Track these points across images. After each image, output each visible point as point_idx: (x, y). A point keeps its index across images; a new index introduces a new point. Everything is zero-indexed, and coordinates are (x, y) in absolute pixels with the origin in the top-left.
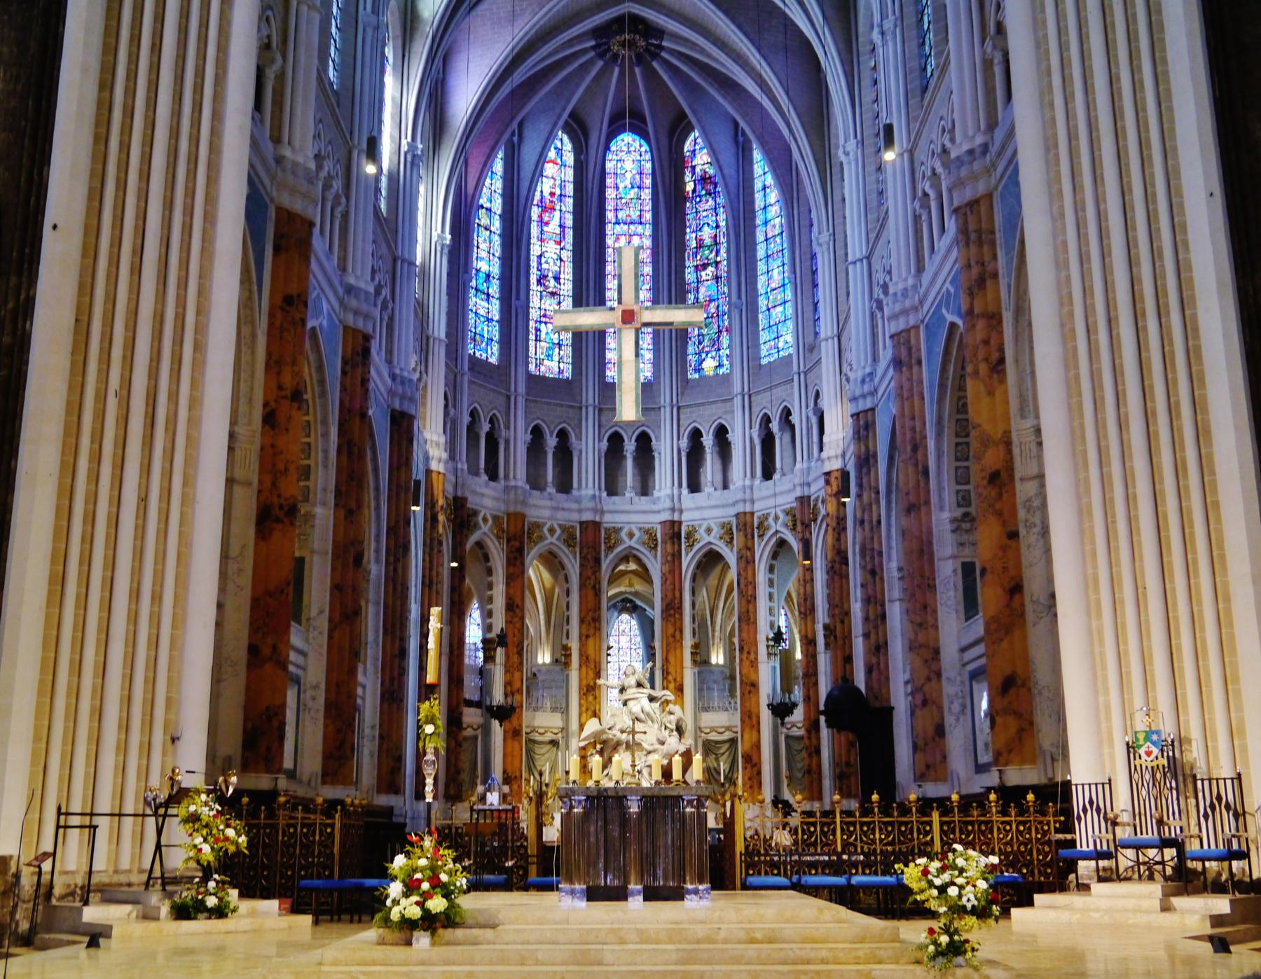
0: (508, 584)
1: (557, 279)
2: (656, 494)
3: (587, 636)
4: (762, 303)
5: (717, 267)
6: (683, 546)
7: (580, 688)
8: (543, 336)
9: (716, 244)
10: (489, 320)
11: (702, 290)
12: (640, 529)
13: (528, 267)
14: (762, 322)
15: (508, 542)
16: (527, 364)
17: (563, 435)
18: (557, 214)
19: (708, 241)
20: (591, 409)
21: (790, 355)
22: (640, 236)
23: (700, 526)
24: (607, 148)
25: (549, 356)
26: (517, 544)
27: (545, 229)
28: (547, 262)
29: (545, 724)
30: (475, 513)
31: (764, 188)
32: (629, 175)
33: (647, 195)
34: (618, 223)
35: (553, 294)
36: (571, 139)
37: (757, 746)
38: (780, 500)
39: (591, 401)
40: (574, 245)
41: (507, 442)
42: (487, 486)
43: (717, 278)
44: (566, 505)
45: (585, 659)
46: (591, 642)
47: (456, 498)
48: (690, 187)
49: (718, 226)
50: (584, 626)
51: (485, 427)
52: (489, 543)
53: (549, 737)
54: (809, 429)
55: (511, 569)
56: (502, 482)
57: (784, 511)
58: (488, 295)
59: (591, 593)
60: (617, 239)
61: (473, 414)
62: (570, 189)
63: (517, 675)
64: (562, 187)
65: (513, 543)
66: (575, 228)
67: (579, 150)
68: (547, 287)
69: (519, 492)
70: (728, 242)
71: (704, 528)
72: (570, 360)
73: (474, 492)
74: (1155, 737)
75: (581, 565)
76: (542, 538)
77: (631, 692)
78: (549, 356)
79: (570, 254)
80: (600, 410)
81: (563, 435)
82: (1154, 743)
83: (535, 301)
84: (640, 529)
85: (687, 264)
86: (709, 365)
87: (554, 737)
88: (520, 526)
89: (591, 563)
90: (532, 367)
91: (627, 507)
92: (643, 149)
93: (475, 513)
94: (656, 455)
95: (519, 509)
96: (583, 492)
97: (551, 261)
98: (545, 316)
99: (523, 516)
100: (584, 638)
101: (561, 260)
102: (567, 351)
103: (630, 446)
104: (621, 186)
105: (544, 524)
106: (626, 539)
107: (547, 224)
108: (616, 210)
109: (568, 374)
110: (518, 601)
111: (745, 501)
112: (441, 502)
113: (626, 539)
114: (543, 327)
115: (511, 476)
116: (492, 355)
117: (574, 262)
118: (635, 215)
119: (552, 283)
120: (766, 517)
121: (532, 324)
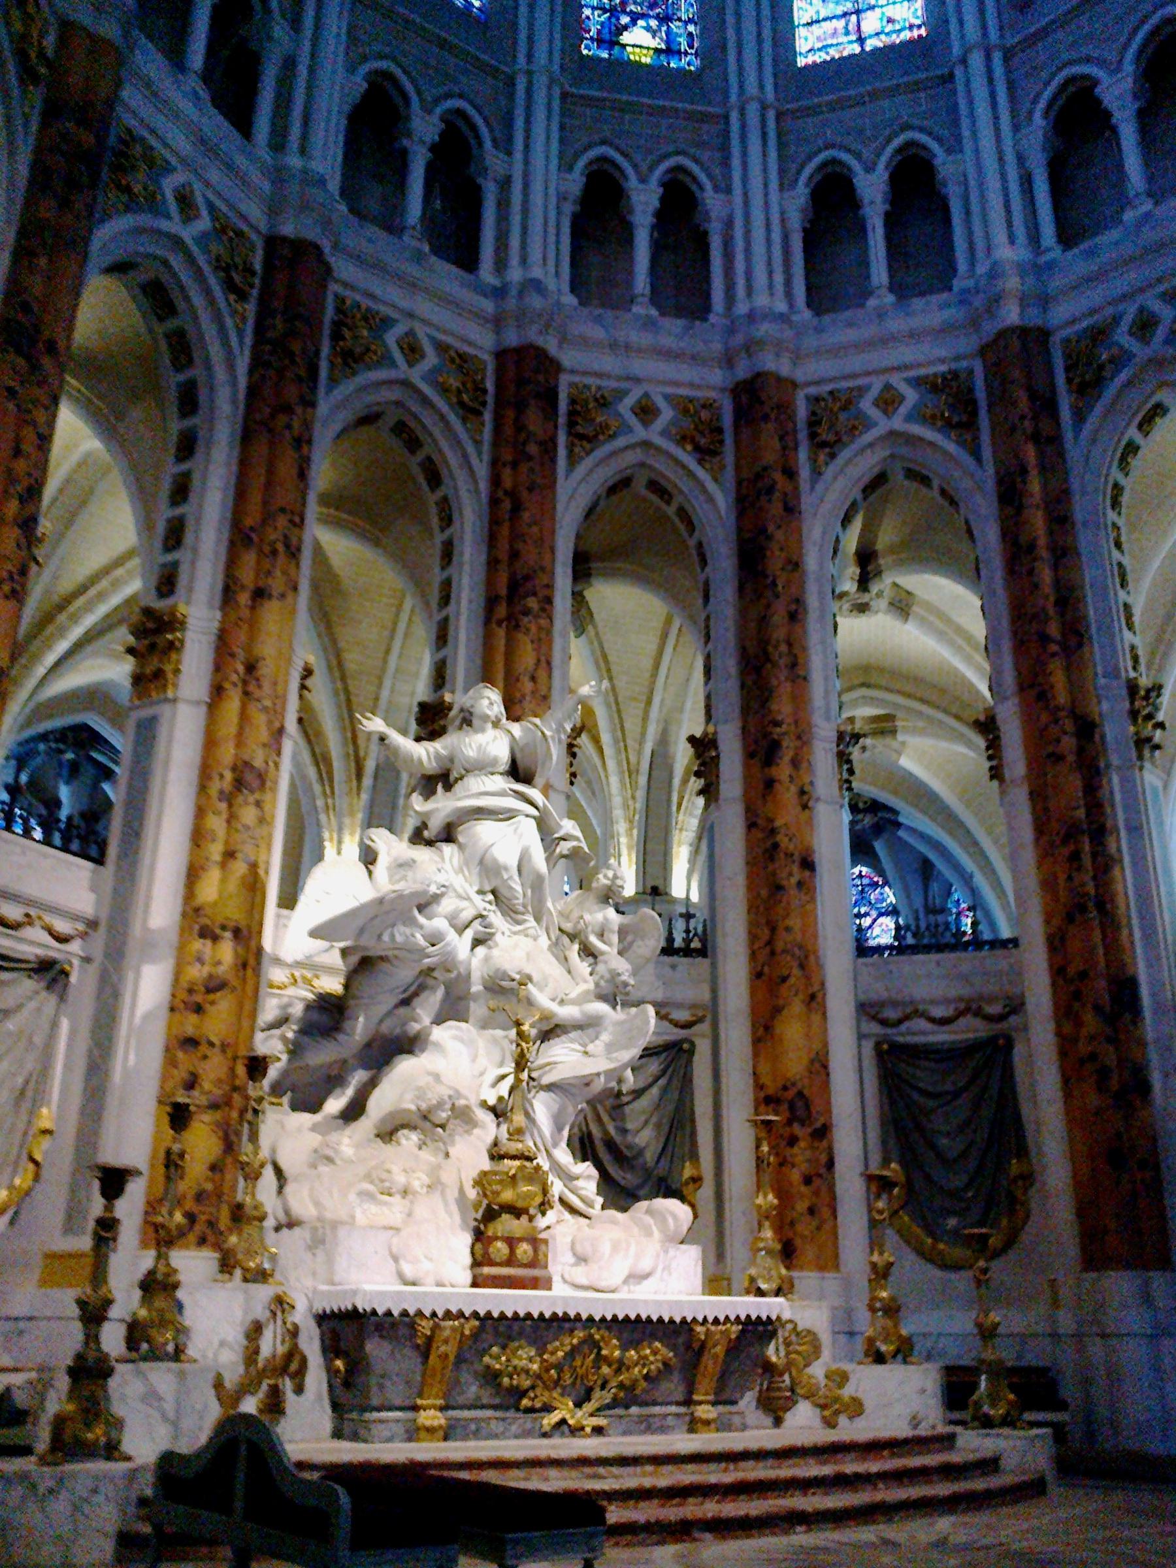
3: (260, 594)
6: (562, 438)
12: (442, 348)
23: (621, 394)
29: (31, 888)
37: (820, 1065)
38: (905, 353)
50: (249, 559)
53: (32, 944)
54: (1027, 181)
57: (917, 382)
71: (630, 401)
77: (488, 788)
87: (54, 950)
111: (779, 347)
120: (847, 401)
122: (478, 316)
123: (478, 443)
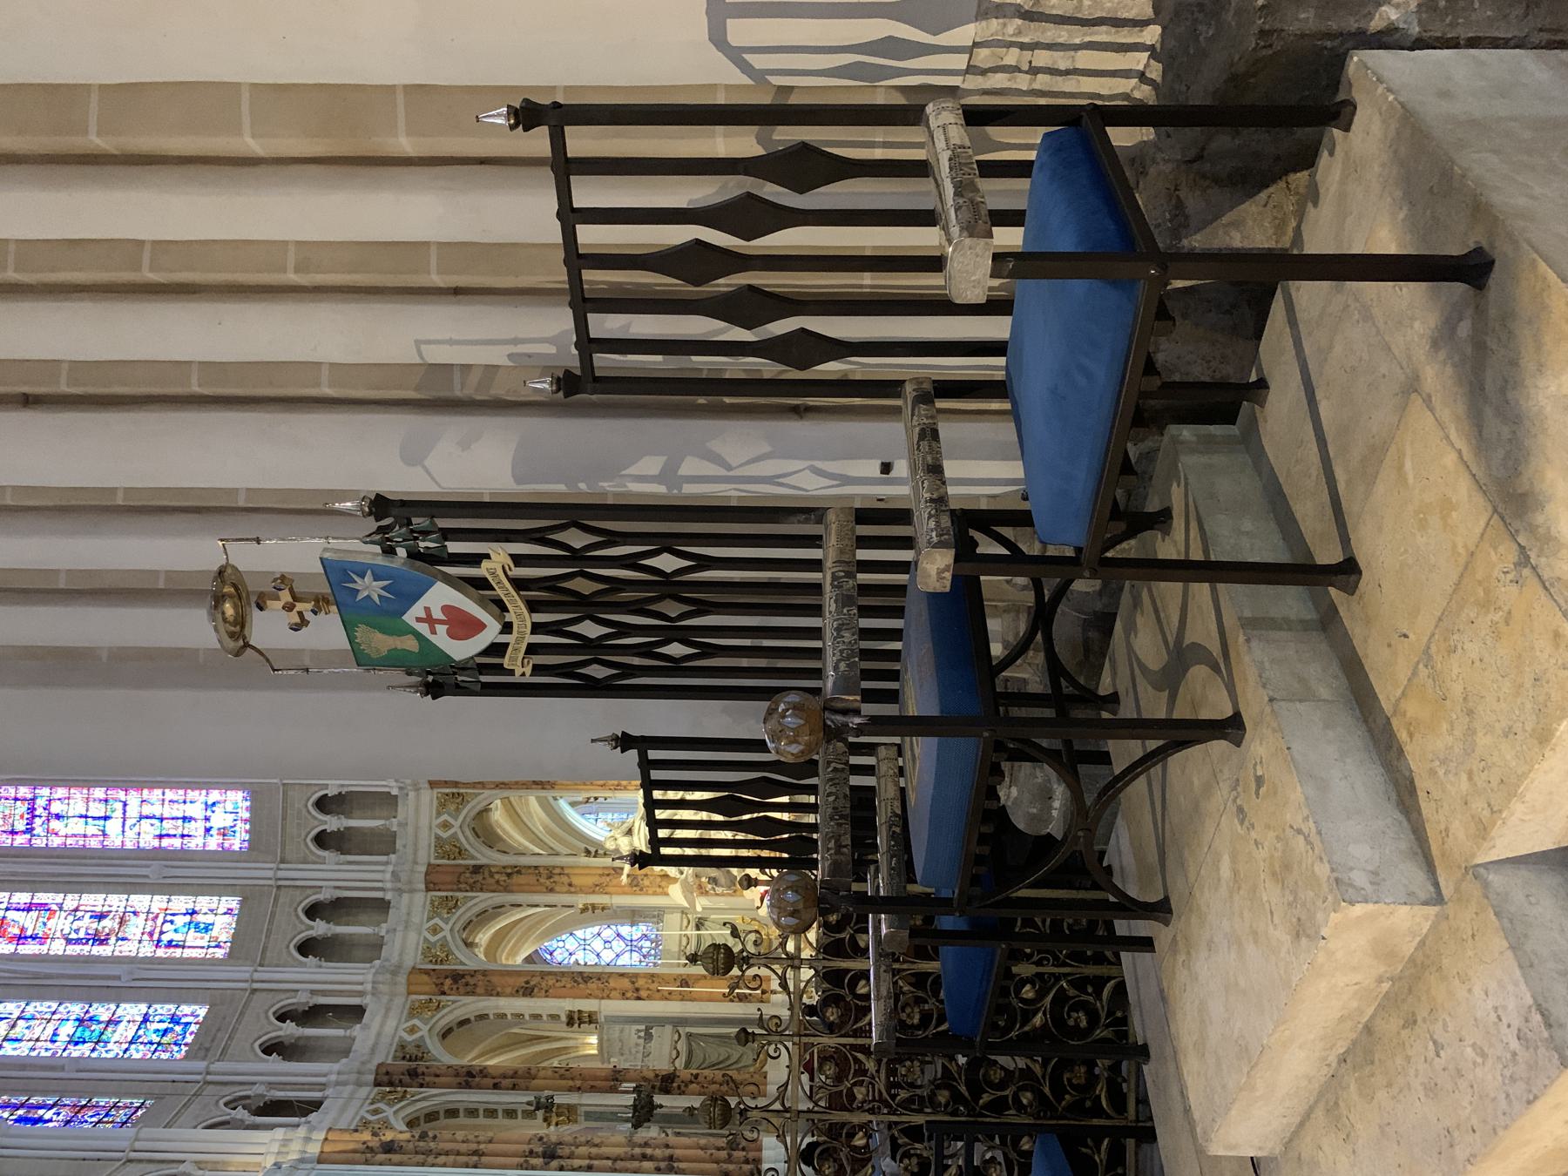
0: (498, 995)
1: (101, 917)
2: (394, 792)
7: (634, 893)
8: (178, 937)
10: (146, 1019)
12: (439, 814)
15: (444, 993)
17: (313, 911)
20: (281, 874)
25: (207, 928)
26: (448, 982)
28: (77, 931)
30: (402, 1046)
34: (30, 830)
35: (122, 922)
39: (270, 874)
41: (313, 992)
42: (367, 1027)
44: (404, 910)
45: (597, 888)
46: (576, 881)
47: (377, 1084)
51: (290, 1029)
52: (443, 1022)
55: (478, 990)
56: (366, 1001)
58: (109, 1022)
59: (516, 879)
61: (268, 1050)
63: (612, 984)
65: (446, 988)
68: (112, 930)
69: (380, 978)
72: (215, 899)
73: (373, 1050)
74: (370, 588)
75: (481, 890)
76: (444, 944)
78: (207, 928)
79: (70, 896)
80: (283, 861)
81: (313, 911)
82: (406, 595)
84: (439, 814)
87: (693, 924)
88: (425, 978)
89: (478, 878)
90: (219, 953)
91: (410, 829)
93: (402, 1046)
94: (344, 790)
95: (402, 979)
96: (389, 885)
97: (76, 925)
98: (151, 934)
99: (414, 971)
100: (571, 888)
101: (76, 910)
102: (203, 902)
103: (332, 823)
105: (426, 940)
106: (450, 832)
109: (233, 902)
110: (521, 981)
112: (366, 1136)
113: (450, 832)
114: (165, 938)
115: (359, 988)
118: (22, 808)
119: (107, 923)
121: (161, 953)
122: (418, 797)
123: (477, 795)
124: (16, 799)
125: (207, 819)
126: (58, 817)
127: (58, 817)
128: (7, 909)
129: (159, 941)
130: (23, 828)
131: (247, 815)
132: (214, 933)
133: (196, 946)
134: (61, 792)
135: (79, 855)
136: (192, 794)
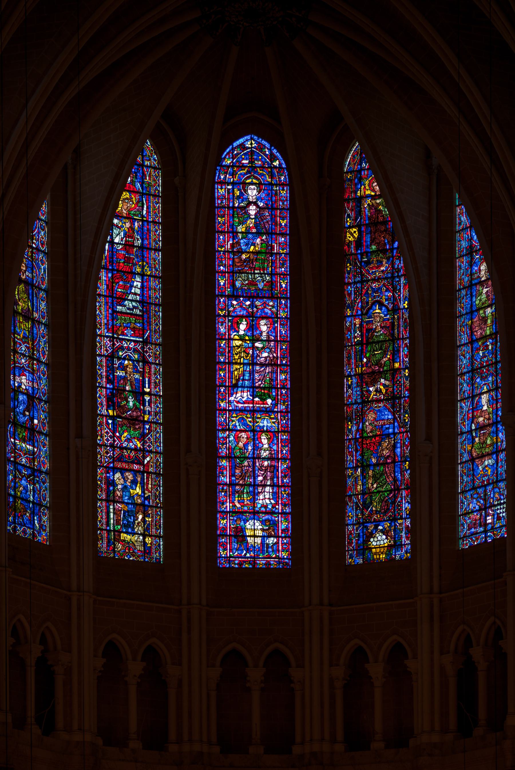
1: (139, 395)
4: (464, 448)
5: (393, 380)
9: (394, 339)
11: (371, 416)
13: (94, 375)
14: (463, 480)
16: (96, 540)
18: (137, 283)
19: (380, 334)
21: (502, 538)
22: (272, 319)
24: (219, 161)
27: (119, 308)
28: (123, 368)
31: (471, 251)
32: (252, 210)
33: (281, 245)
36: (158, 148)
40: (165, 334)
43: (392, 398)
48: (352, 235)
49: (396, 309)
60: (234, 327)
62: (156, 234)
64: (144, 234)
66: (165, 305)
67: (169, 168)
68: (124, 409)
70: (411, 338)
79: (159, 350)
83: (104, 436)
85: (347, 371)
86: (380, 540)
90: (102, 545)
92: (276, 164)
98: (120, 459)
101: (145, 362)
104: (241, 229)
107: (121, 299)
108: (232, 273)
116: (41, 528)
117: (164, 364)
124: (271, 275)
125: (255, 514)
126: (252, 327)
127: (252, 327)
128: (142, 275)
129: (115, 470)
130: (238, 284)
131: (261, 563)
132: (123, 536)
133: (109, 516)
134: (283, 331)
135: (210, 364)
136: (284, 494)
